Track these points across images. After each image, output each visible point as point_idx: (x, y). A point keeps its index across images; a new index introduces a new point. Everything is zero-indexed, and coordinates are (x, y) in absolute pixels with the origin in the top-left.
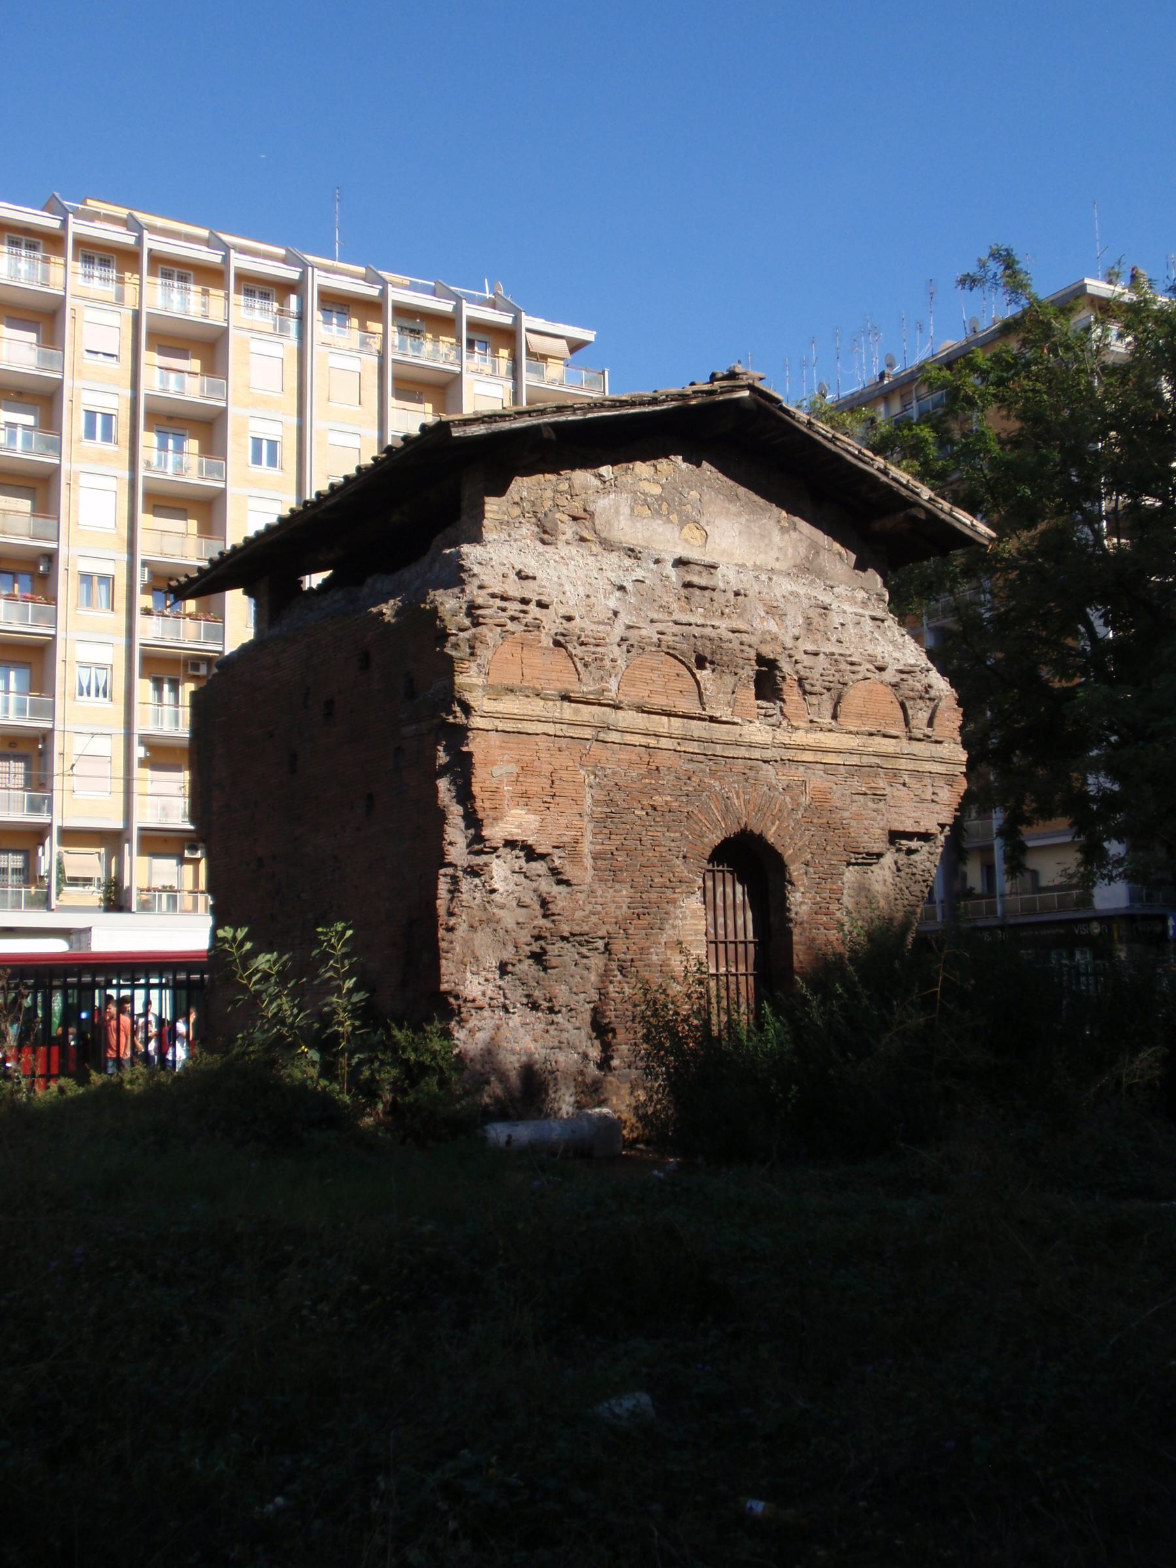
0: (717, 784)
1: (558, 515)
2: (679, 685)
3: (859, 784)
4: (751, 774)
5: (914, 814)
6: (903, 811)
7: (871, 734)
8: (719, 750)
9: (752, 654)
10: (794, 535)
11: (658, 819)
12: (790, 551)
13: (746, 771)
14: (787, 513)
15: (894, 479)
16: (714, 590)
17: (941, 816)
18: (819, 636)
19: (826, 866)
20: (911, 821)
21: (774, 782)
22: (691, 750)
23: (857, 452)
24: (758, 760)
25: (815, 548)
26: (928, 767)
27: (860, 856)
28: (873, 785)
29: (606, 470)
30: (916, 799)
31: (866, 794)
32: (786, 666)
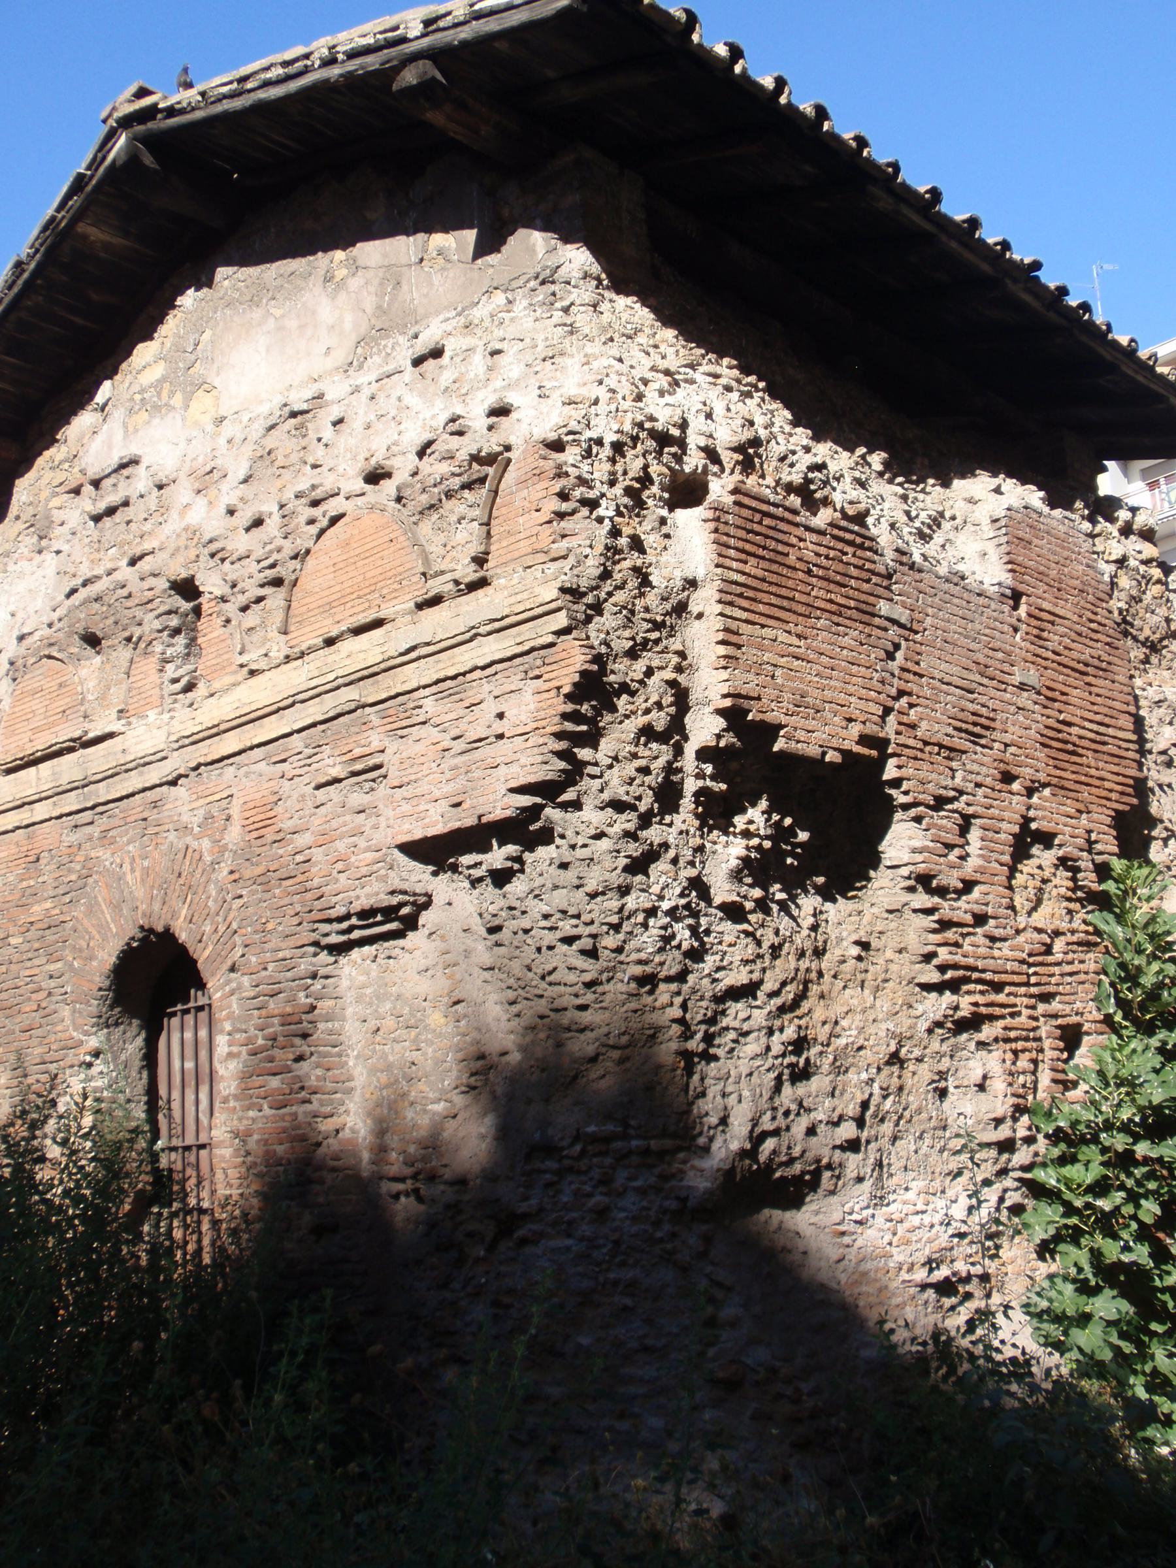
0: (108, 855)
1: (56, 502)
2: (62, 703)
3: (330, 761)
4: (153, 816)
5: (448, 789)
6: (423, 787)
7: (330, 642)
8: (103, 792)
9: (162, 584)
10: (354, 283)
11: (36, 945)
12: (349, 319)
13: (145, 815)
14: (344, 249)
15: (352, 55)
16: (126, 504)
17: (514, 769)
18: (287, 475)
19: (271, 967)
20: (443, 805)
21: (185, 818)
22: (67, 810)
23: (280, 71)
24: (161, 785)
25: (393, 278)
26: (465, 658)
27: (345, 925)
28: (358, 752)
29: (105, 390)
30: (460, 745)
31: (337, 781)
32: (211, 583)
